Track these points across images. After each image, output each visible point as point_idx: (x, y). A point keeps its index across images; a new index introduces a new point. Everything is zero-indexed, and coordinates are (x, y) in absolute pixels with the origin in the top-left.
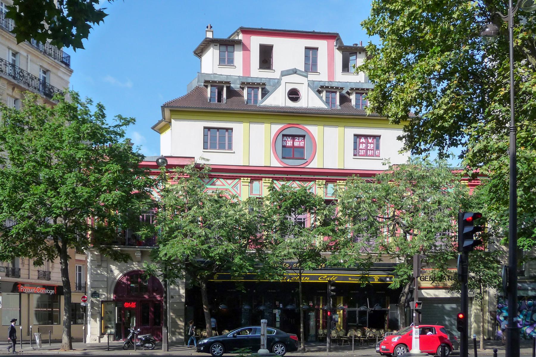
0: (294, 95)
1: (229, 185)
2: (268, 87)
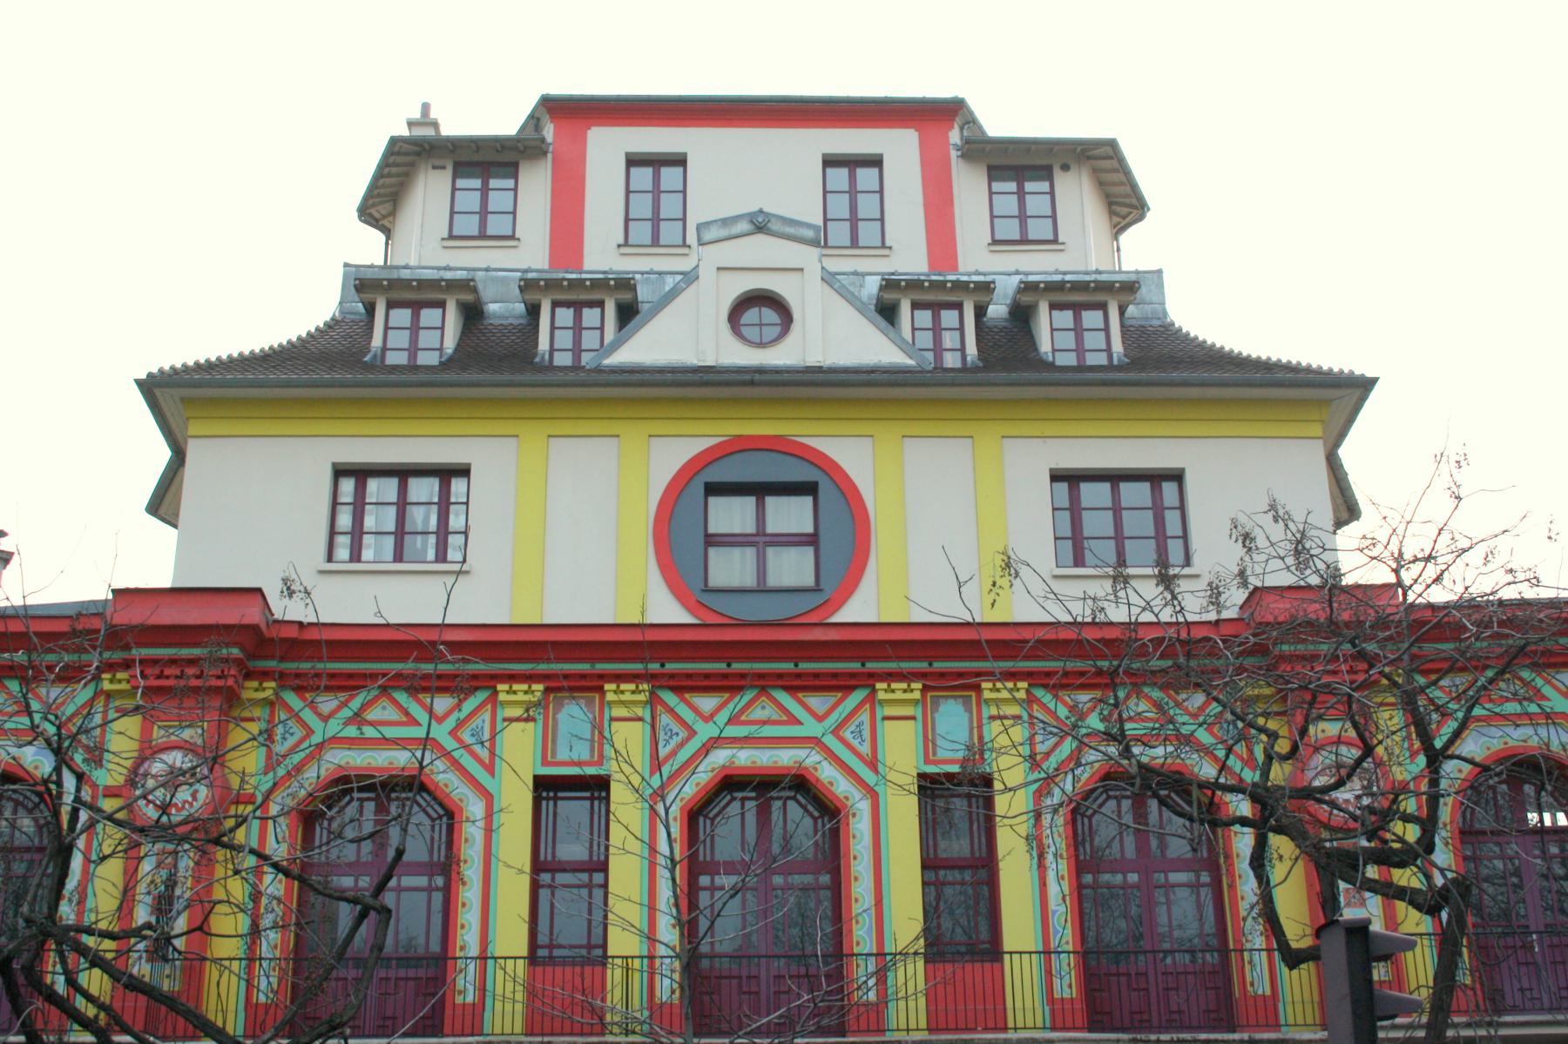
2: (643, 293)
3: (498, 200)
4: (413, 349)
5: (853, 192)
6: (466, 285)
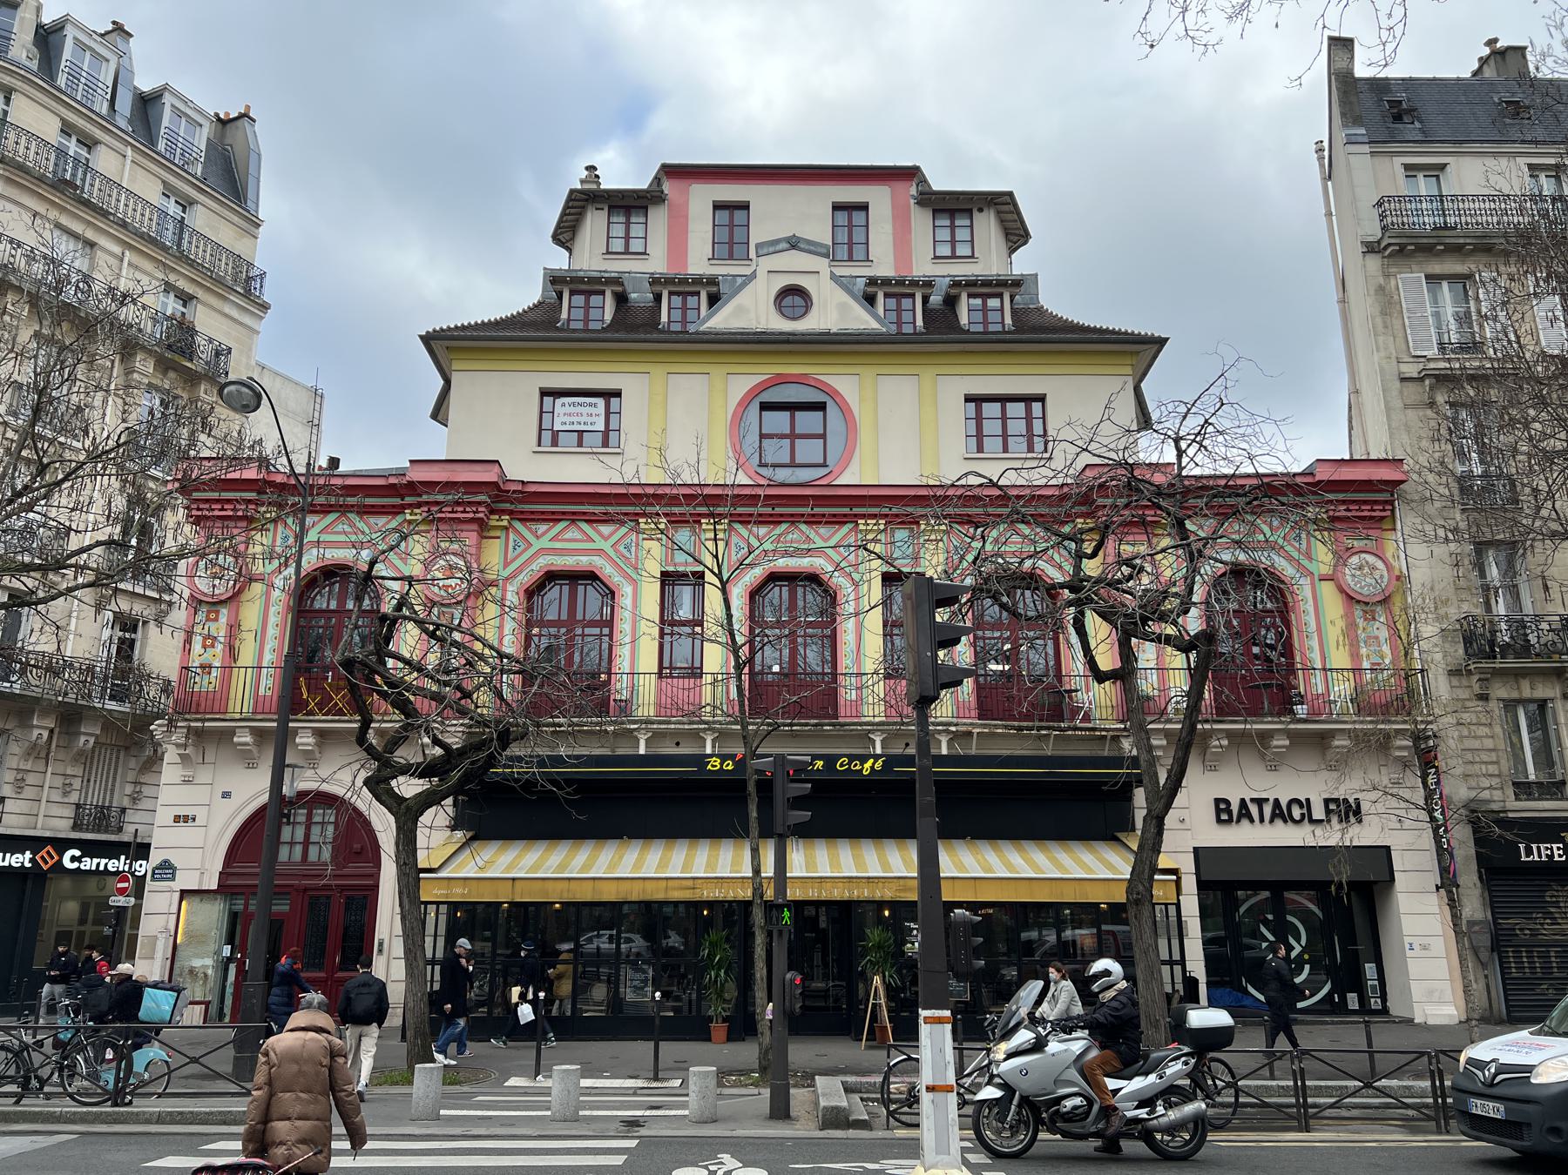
0: (793, 297)
1: (606, 539)
2: (723, 288)
3: (636, 230)
4: (586, 320)
5: (850, 226)
6: (616, 281)
